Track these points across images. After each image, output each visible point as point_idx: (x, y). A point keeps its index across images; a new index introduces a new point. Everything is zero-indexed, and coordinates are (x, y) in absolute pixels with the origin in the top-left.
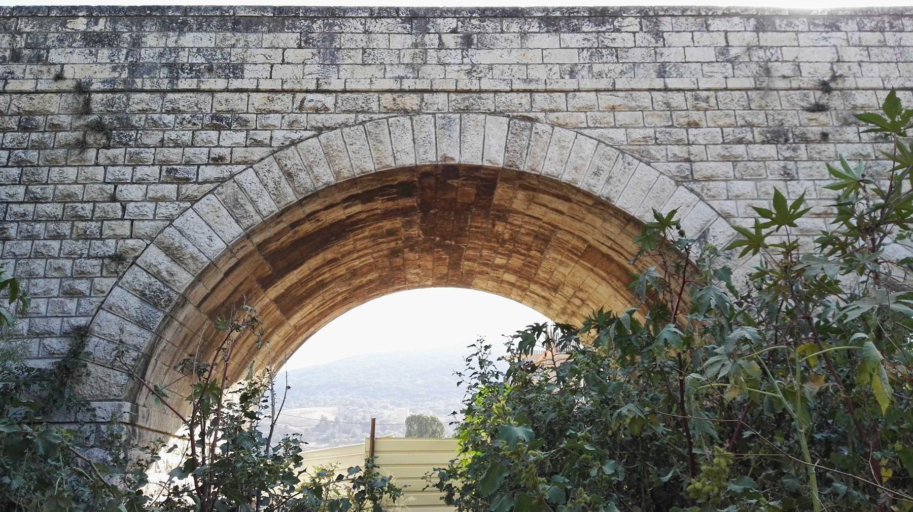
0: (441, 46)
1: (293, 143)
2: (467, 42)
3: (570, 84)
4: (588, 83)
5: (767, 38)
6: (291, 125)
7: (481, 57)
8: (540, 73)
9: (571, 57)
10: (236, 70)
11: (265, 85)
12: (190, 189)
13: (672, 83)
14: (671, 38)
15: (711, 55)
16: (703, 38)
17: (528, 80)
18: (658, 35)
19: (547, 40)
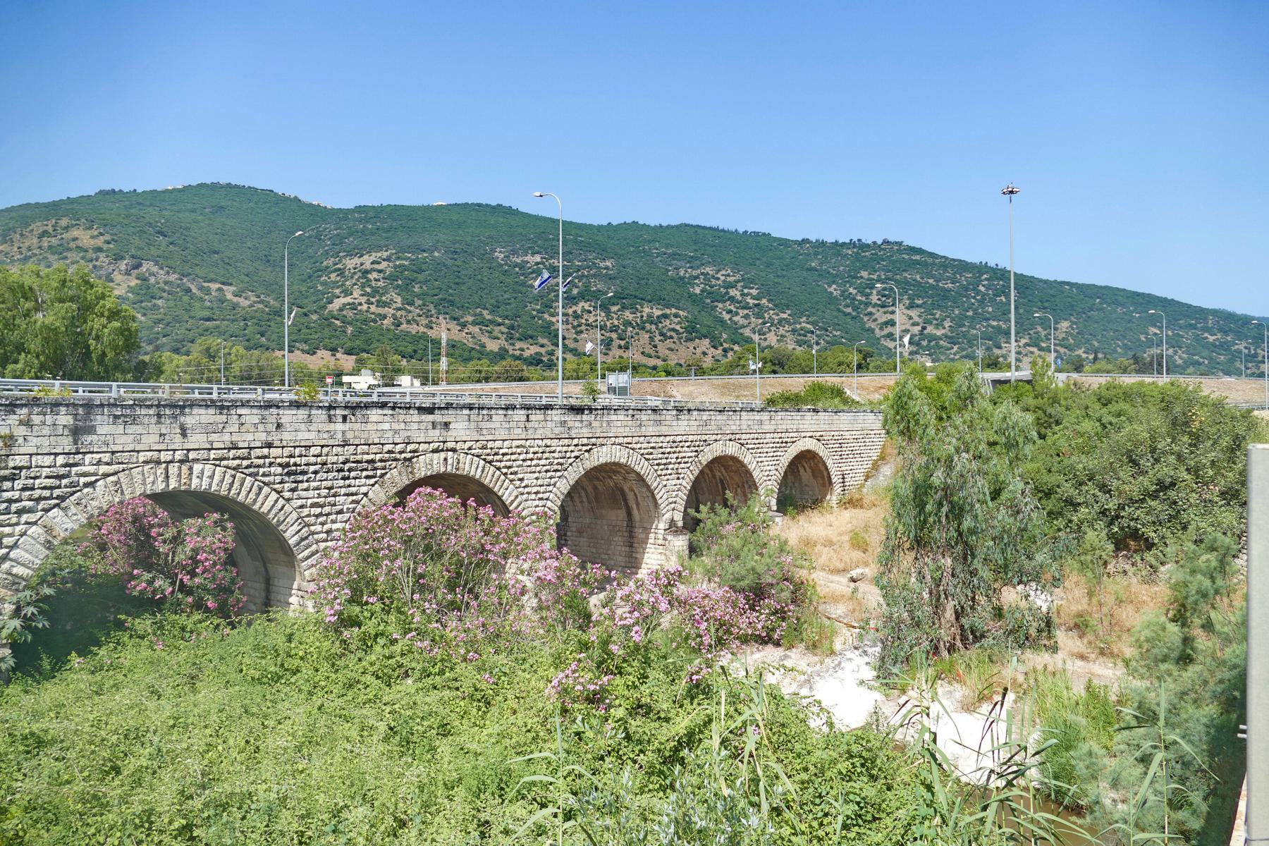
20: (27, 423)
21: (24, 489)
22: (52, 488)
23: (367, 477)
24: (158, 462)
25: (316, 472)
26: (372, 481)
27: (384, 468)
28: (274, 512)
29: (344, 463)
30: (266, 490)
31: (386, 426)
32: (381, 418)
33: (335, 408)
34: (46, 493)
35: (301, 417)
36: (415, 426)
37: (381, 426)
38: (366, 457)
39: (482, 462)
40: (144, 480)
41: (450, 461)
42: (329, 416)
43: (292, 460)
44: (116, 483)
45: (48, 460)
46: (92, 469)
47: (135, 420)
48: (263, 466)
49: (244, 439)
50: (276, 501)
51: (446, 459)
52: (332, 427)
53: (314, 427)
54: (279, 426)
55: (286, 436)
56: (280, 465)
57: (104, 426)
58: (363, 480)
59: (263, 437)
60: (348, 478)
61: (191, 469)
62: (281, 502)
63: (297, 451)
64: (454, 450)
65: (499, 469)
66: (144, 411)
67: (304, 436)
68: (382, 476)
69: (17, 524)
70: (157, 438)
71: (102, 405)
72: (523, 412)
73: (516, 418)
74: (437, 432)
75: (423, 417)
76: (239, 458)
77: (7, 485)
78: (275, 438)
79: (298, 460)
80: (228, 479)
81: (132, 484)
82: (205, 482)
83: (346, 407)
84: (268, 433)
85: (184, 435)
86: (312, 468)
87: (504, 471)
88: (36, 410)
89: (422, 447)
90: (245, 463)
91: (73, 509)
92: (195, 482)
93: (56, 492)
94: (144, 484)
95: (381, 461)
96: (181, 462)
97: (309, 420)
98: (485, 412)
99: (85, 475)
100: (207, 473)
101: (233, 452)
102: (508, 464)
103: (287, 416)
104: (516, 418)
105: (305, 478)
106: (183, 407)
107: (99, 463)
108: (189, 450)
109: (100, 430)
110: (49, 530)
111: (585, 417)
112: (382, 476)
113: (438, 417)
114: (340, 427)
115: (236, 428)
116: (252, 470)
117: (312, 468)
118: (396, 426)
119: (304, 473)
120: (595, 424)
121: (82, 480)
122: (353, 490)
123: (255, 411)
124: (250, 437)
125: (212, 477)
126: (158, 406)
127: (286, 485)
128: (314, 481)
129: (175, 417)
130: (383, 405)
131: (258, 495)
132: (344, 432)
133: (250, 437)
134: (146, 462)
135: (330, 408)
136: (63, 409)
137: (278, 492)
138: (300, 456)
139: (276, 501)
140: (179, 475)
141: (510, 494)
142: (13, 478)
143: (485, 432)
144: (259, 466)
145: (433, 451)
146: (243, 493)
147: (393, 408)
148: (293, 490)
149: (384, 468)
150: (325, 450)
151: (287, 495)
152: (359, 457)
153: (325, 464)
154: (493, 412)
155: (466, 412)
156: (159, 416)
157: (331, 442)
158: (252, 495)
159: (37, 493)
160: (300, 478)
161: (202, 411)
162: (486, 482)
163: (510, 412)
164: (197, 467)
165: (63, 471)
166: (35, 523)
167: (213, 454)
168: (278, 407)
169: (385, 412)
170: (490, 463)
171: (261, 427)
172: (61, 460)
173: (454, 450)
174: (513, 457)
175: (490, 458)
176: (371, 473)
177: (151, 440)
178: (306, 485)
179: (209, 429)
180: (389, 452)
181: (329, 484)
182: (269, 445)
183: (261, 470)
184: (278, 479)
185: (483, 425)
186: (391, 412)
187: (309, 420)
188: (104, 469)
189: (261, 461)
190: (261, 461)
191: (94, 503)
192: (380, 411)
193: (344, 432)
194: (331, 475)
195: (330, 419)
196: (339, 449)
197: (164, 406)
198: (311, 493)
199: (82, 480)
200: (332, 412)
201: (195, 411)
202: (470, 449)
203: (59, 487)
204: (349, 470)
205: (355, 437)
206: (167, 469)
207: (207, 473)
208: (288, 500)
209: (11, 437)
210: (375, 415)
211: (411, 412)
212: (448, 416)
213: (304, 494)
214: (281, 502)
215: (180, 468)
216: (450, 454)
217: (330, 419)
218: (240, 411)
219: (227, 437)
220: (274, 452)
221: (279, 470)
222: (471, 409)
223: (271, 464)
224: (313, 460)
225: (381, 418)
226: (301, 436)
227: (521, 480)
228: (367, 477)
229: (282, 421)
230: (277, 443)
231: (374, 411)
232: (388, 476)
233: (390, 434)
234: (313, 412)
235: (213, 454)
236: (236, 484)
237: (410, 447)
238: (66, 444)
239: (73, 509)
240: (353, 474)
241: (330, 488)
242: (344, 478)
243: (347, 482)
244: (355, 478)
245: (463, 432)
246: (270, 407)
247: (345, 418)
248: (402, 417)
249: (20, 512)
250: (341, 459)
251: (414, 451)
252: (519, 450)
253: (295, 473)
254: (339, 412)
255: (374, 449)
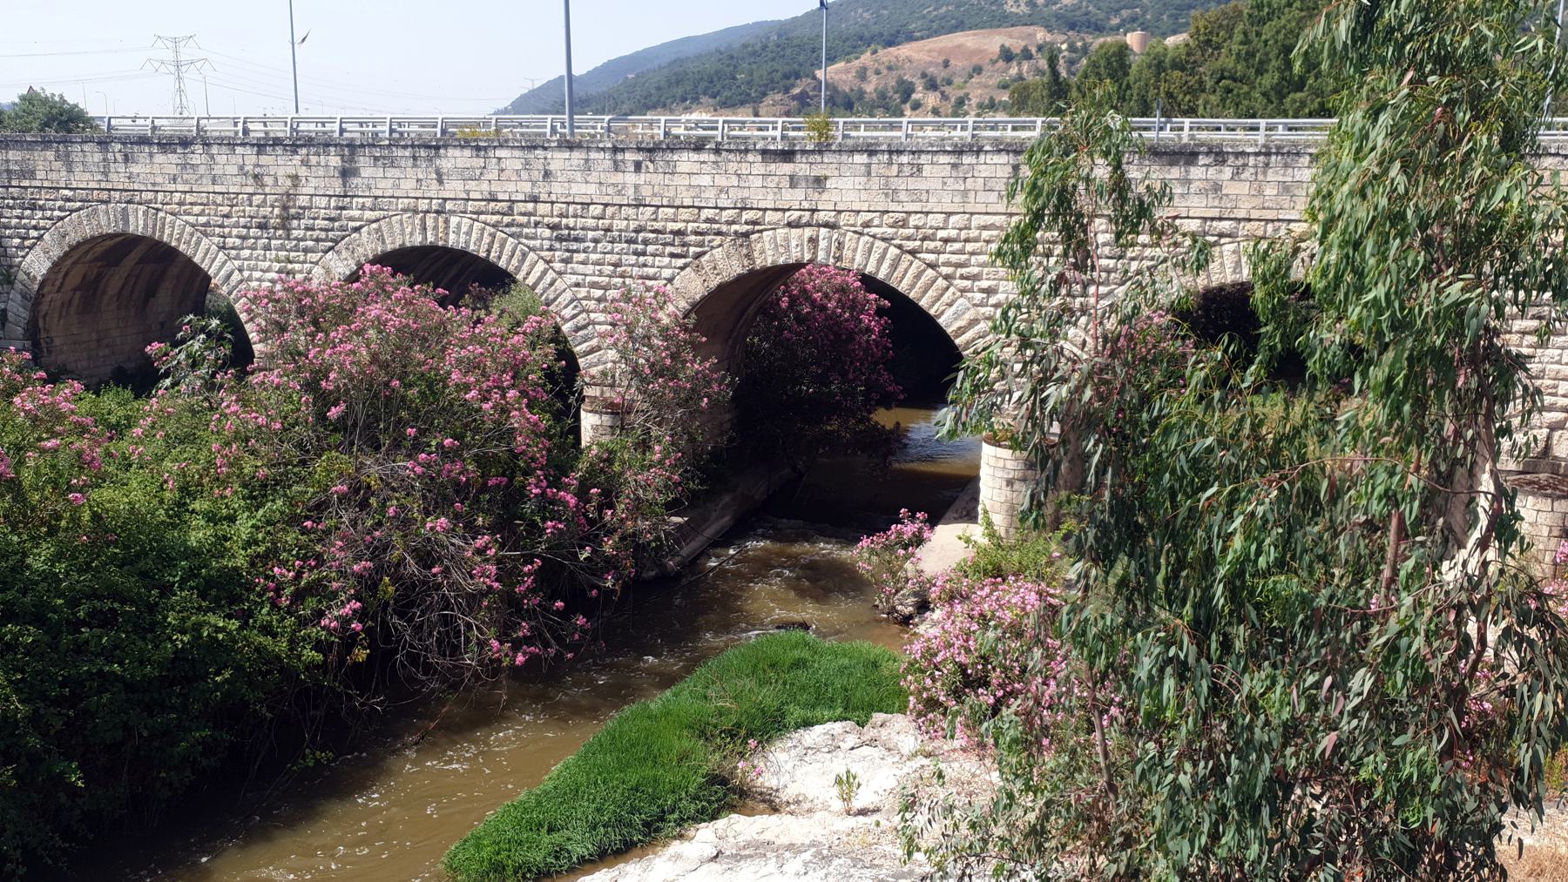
0: (115, 161)
1: (62, 219)
2: (126, 159)
3: (172, 187)
4: (180, 188)
5: (264, 159)
6: (60, 209)
7: (135, 169)
8: (159, 180)
9: (173, 170)
10: (32, 174)
11: (46, 184)
12: (27, 243)
13: (218, 189)
14: (218, 158)
15: (235, 170)
16: (233, 159)
17: (154, 184)
18: (212, 157)
19: (159, 158)
20: (305, 163)
21: (307, 229)
22: (327, 230)
23: (672, 255)
24: (416, 212)
25: (596, 241)
26: (680, 262)
27: (701, 244)
28: (541, 286)
29: (637, 231)
30: (532, 256)
31: (705, 180)
32: (696, 168)
33: (623, 150)
34: (323, 235)
35: (575, 162)
36: (758, 182)
37: (696, 180)
38: (671, 226)
39: (893, 251)
40: (403, 230)
41: (823, 244)
42: (615, 162)
43: (564, 221)
44: (378, 230)
45: (323, 202)
46: (356, 213)
47: (392, 163)
48: (527, 225)
49: (505, 190)
50: (544, 273)
51: (813, 241)
52: (618, 178)
53: (594, 177)
54: (547, 174)
55: (557, 188)
56: (548, 226)
57: (367, 169)
58: (667, 260)
59: (527, 187)
60: (644, 254)
61: (447, 221)
62: (550, 275)
63: (571, 208)
64: (832, 226)
65: (932, 266)
66: (400, 152)
67: (583, 190)
68: (698, 256)
69: (304, 262)
70: (413, 184)
71: (362, 146)
72: (1003, 158)
73: (984, 171)
74: (799, 193)
75: (773, 166)
76: (498, 213)
77: (295, 223)
78: (542, 190)
79: (571, 222)
80: (486, 239)
81: (392, 234)
82: (463, 238)
83: (639, 149)
84: (534, 183)
85: (440, 181)
86: (591, 234)
87: (945, 270)
88: (313, 150)
89: (770, 217)
90: (507, 219)
91: (345, 254)
92: (452, 237)
93: (331, 234)
94: (403, 234)
95: (697, 233)
96: (437, 212)
97: (587, 166)
98: (905, 159)
99: (351, 219)
100: (464, 229)
101: (492, 204)
102: (954, 258)
103: (559, 160)
104: (984, 171)
105: (582, 246)
106: (437, 148)
107: (363, 208)
108: (445, 200)
109: (365, 172)
110: (328, 272)
111: (1196, 172)
112: (698, 256)
113: (801, 167)
114: (631, 178)
115: (493, 175)
116: (514, 229)
117: (591, 234)
118: (721, 181)
119: (576, 240)
120: (1230, 189)
121: (351, 224)
122: (651, 271)
123: (517, 153)
124: (511, 187)
125: (469, 233)
126: (413, 146)
127: (557, 253)
128: (595, 251)
129: (430, 159)
130: (699, 146)
131: (522, 261)
132: (637, 187)
133: (511, 187)
134: (405, 210)
135: (615, 150)
136: (332, 149)
137: (548, 262)
138: (575, 216)
139: (544, 273)
140: (436, 228)
141: (957, 316)
142: (298, 217)
143: (903, 196)
144: (521, 225)
145: (790, 225)
146: (504, 258)
147: (717, 151)
148: (566, 261)
149: (701, 244)
150: (610, 210)
151: (558, 266)
152: (658, 225)
153: (608, 230)
154: (924, 159)
155: (861, 159)
156: (415, 158)
157: (617, 200)
158: (514, 262)
159: (315, 234)
160: (574, 246)
161: (457, 152)
162: (902, 287)
163: (967, 159)
164: (454, 220)
165: (334, 213)
166: (317, 263)
167: (471, 206)
168: (545, 149)
169: (704, 157)
170: (913, 252)
171: (524, 175)
172: (333, 203)
173: (832, 226)
174: (970, 247)
175: (910, 245)
176: (678, 250)
177: (408, 185)
178: (582, 256)
179: (467, 176)
180: (708, 220)
181: (614, 258)
182: (535, 200)
183: (526, 230)
184: (546, 244)
185: (900, 184)
186: (713, 157)
187: (587, 166)
188: (368, 214)
189: (524, 219)
190: (524, 219)
191: (361, 250)
192: (694, 156)
193: (637, 187)
194: (618, 247)
195: (617, 166)
196: (631, 211)
197: (419, 146)
198: (590, 269)
199: (351, 224)
200: (619, 157)
201: (451, 152)
202: (867, 225)
203: (332, 230)
204: (646, 242)
205: (654, 195)
206: (423, 221)
207: (464, 229)
208: (560, 273)
209: (297, 177)
210: (686, 161)
211: (750, 157)
212: (826, 165)
213: (580, 268)
214: (550, 275)
215: (436, 220)
216: (823, 231)
217: (617, 166)
218: (501, 153)
219: (485, 186)
220: (543, 208)
221: (547, 233)
222: (872, 153)
223: (537, 224)
224: (591, 222)
225: (696, 168)
226: (575, 189)
227: (989, 291)
228: (672, 255)
229: (551, 167)
230: (544, 197)
231: (685, 155)
232: (706, 257)
233: (711, 193)
234: (593, 155)
235: (471, 206)
236: (496, 245)
237: (747, 216)
238: (337, 186)
239: (345, 254)
240: (650, 249)
241: (616, 265)
242: (636, 253)
243: (642, 259)
244: (654, 255)
245: (852, 196)
246: (535, 148)
247: (638, 166)
248: (732, 167)
249: (306, 251)
250: (633, 225)
251: (755, 223)
252: (985, 234)
253: (568, 239)
254: (630, 157)
255: (684, 214)
